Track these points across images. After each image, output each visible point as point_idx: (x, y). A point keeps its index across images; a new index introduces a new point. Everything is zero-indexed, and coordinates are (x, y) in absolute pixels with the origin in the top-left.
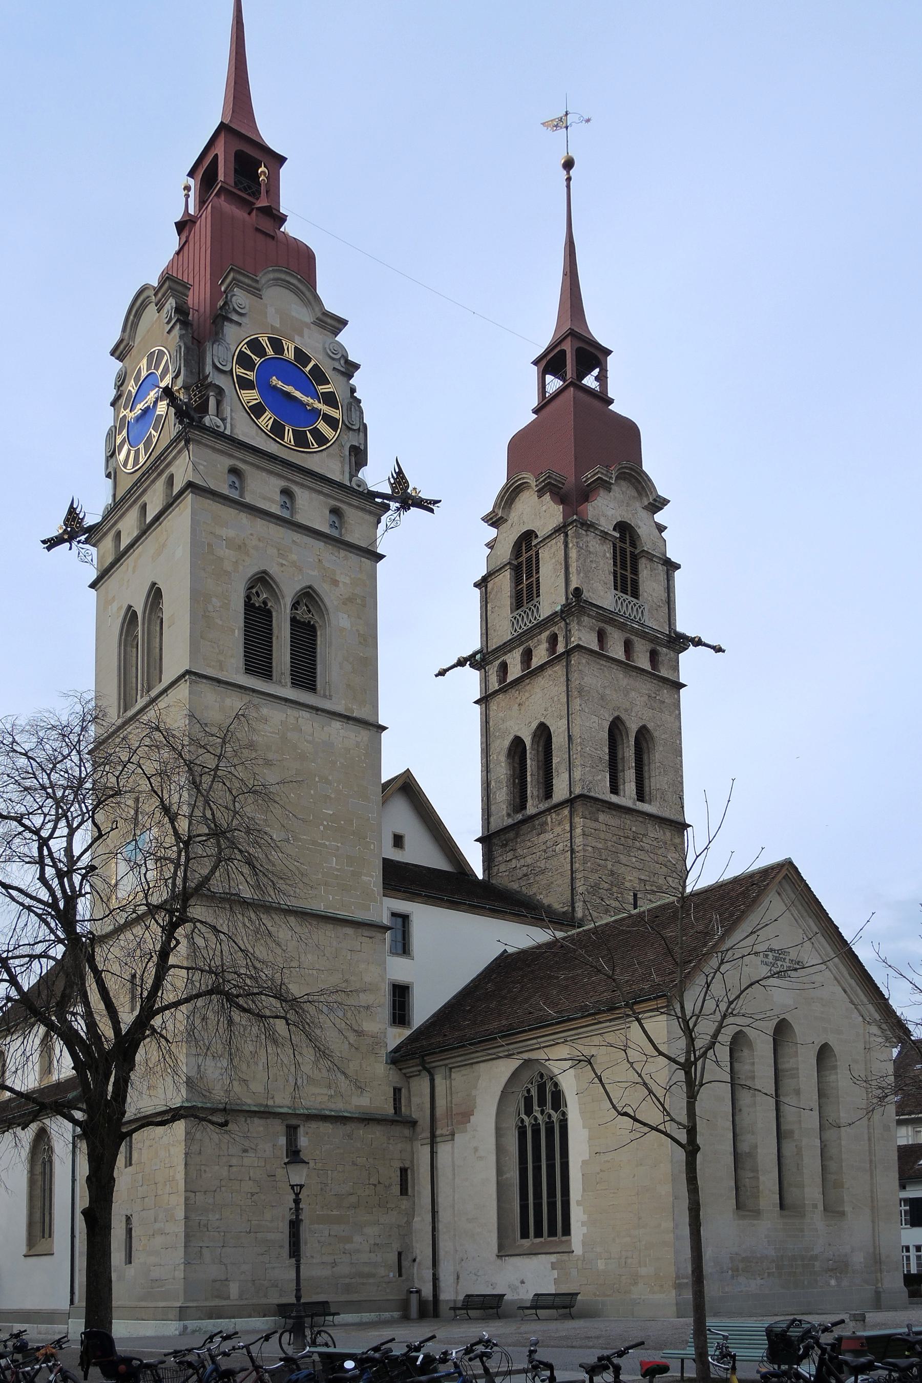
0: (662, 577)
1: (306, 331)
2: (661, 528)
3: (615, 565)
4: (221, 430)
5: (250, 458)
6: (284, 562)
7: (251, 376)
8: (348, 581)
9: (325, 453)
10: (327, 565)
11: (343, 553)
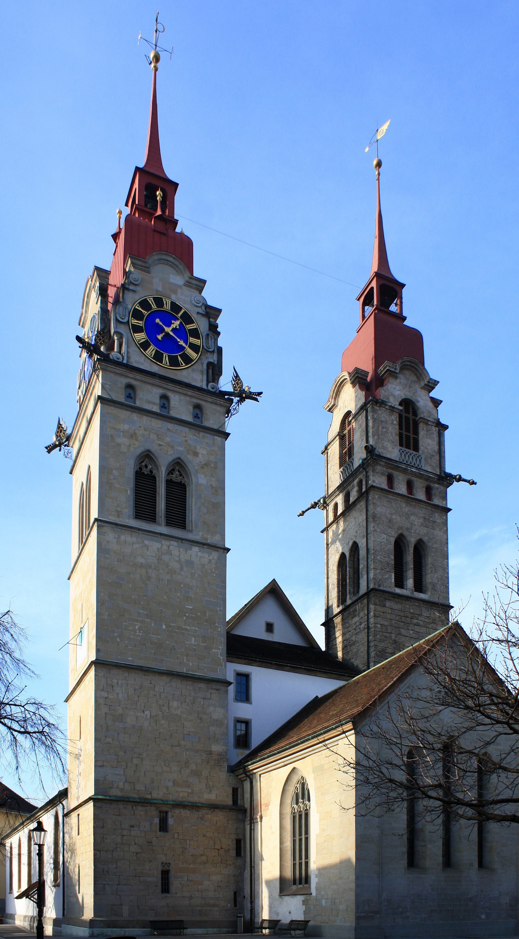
0: (435, 436)
1: (179, 290)
2: (436, 403)
3: (400, 428)
4: (121, 360)
5: (139, 376)
6: (162, 443)
7: (141, 323)
8: (204, 452)
9: (190, 369)
10: (190, 442)
11: (202, 434)
